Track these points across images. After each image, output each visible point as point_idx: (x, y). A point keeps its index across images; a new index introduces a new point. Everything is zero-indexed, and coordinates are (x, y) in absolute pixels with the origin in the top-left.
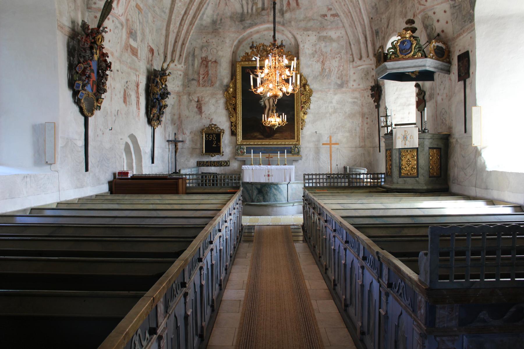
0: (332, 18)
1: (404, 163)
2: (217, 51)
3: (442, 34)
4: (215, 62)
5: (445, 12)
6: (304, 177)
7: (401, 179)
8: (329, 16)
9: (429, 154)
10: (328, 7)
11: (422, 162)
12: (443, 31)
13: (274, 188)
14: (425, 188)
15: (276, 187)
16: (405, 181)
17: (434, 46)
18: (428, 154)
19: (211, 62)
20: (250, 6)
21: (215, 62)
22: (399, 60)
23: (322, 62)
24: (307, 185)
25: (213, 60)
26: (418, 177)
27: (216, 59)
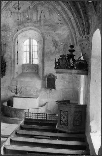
0: (61, 25)
1: (62, 117)
2: (6, 39)
3: (85, 54)
4: (5, 44)
5: (86, 44)
6: (25, 114)
7: (61, 125)
8: (59, 24)
9: (74, 115)
10: (59, 20)
11: (70, 118)
12: (86, 54)
13: (22, 111)
14: (70, 132)
15: (22, 111)
16: (62, 126)
17: (77, 63)
18: (73, 115)
19: (3, 45)
20: (22, 18)
21: (5, 44)
22: (61, 68)
23: (56, 46)
24: (26, 118)
25: (4, 44)
26: (67, 125)
27: (5, 43)
